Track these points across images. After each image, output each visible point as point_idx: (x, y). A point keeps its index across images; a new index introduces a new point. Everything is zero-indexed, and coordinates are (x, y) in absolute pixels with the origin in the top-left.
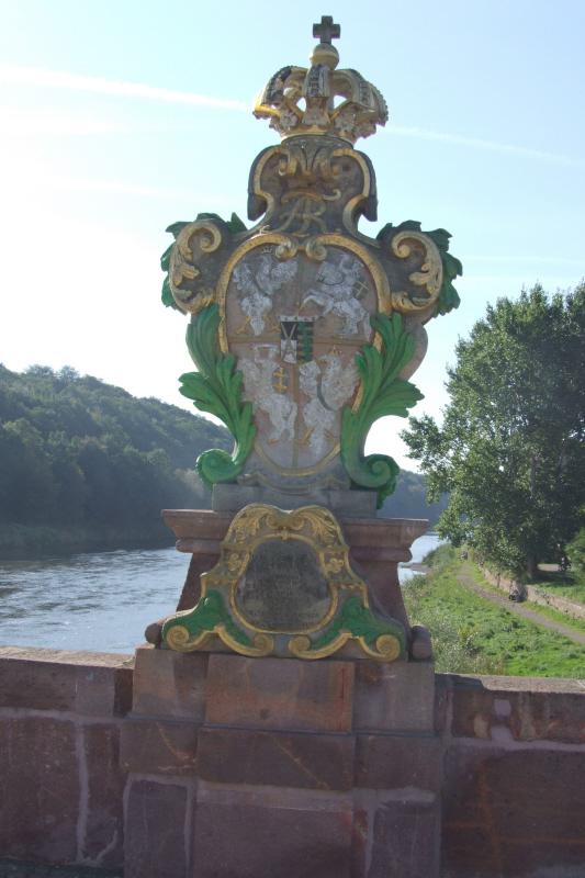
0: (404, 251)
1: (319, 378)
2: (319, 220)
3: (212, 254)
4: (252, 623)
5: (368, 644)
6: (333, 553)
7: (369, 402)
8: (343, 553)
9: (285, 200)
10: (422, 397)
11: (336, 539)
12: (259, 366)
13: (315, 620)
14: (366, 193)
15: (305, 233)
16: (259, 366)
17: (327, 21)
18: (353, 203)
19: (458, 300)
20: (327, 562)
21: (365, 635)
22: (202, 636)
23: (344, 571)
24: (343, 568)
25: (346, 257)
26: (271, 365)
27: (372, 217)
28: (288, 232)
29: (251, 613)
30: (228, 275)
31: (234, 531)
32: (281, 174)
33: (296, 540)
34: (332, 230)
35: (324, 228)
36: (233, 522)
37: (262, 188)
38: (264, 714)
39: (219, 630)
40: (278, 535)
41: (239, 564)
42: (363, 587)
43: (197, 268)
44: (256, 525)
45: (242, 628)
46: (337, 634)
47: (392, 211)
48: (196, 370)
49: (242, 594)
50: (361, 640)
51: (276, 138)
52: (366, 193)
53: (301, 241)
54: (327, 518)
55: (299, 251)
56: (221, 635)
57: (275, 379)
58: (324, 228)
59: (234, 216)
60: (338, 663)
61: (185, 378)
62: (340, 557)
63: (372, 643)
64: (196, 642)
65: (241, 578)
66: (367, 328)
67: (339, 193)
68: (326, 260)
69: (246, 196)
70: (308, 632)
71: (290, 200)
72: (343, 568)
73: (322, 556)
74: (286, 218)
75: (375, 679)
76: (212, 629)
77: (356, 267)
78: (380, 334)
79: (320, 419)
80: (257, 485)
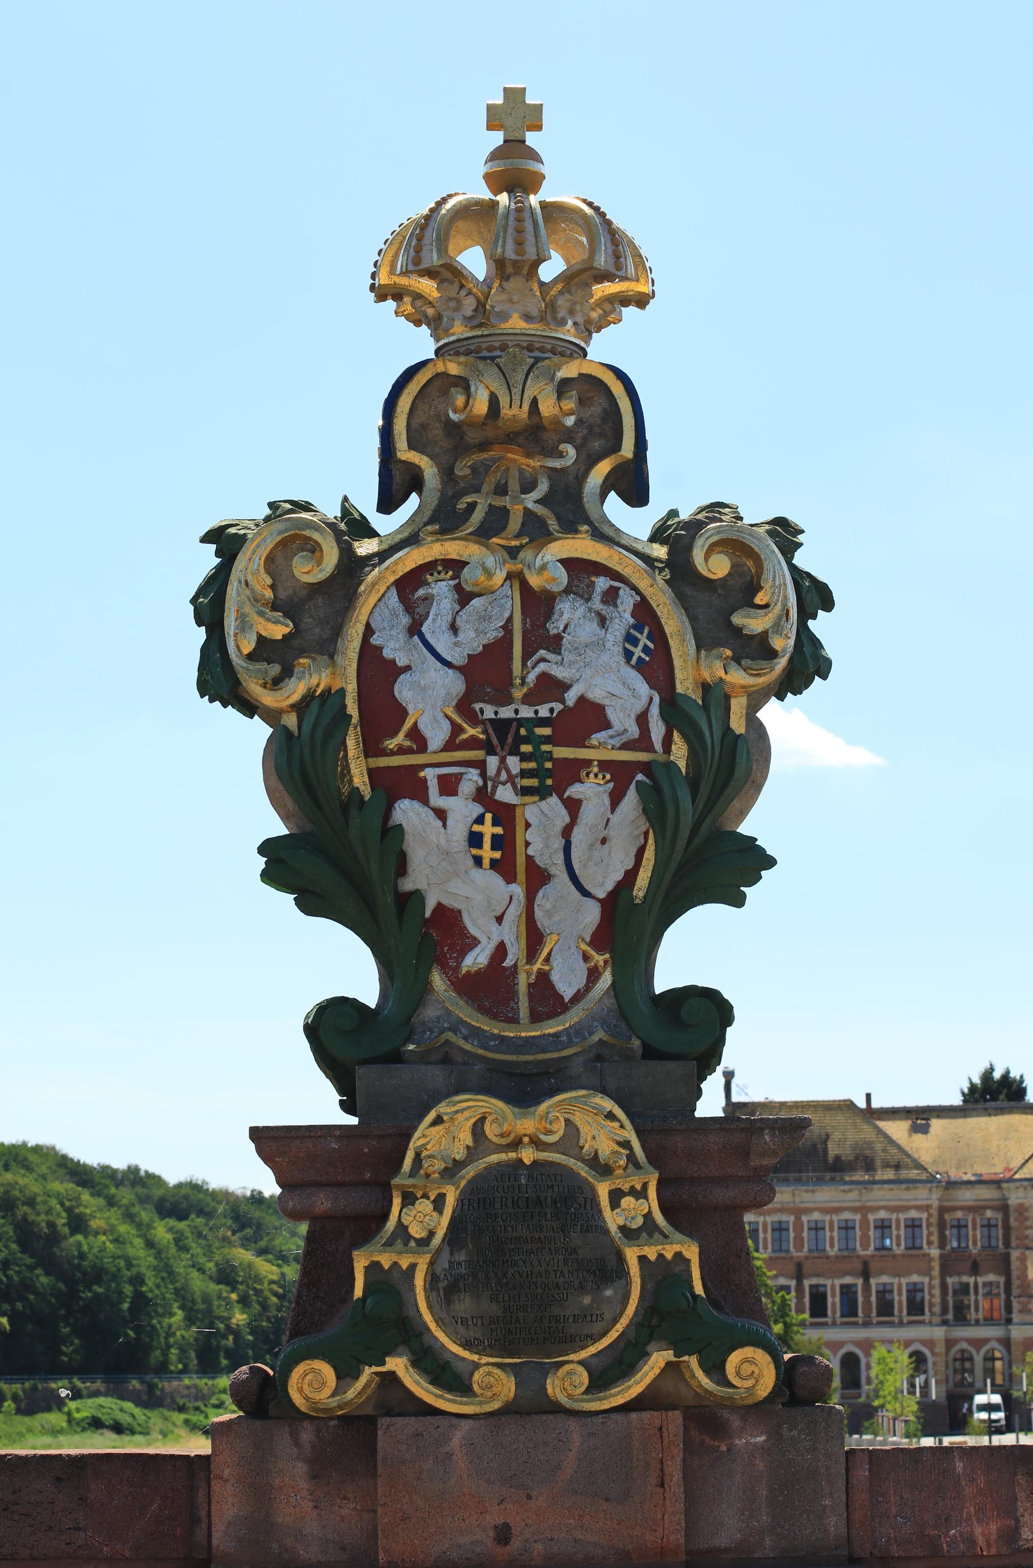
0: (718, 567)
1: (567, 832)
2: (540, 510)
3: (316, 589)
4: (467, 1345)
5: (707, 1372)
6: (626, 1187)
7: (668, 877)
8: (645, 1186)
9: (462, 470)
10: (770, 862)
11: (632, 1158)
12: (441, 814)
13: (597, 1327)
14: (627, 449)
15: (517, 536)
16: (441, 814)
17: (514, 95)
18: (603, 469)
19: (828, 663)
20: (615, 1204)
21: (699, 1352)
22: (363, 1379)
23: (649, 1225)
24: (648, 1216)
25: (602, 583)
26: (462, 809)
27: (637, 494)
28: (484, 534)
29: (464, 1321)
30: (360, 628)
31: (418, 1155)
32: (453, 416)
33: (552, 1164)
34: (570, 528)
35: (553, 524)
36: (418, 1134)
37: (412, 446)
38: (503, 1534)
39: (397, 1364)
40: (512, 1155)
41: (426, 1219)
42: (692, 1252)
43: (286, 615)
44: (466, 1138)
45: (446, 1356)
46: (646, 1355)
47: (677, 486)
48: (284, 831)
49: (441, 1285)
50: (693, 1361)
51: (419, 344)
52: (627, 449)
53: (513, 553)
54: (610, 1116)
55: (509, 576)
56: (401, 1373)
57: (475, 840)
58: (553, 524)
59: (346, 509)
60: (646, 1415)
61: (267, 848)
62: (640, 1194)
63: (716, 1369)
64: (351, 1394)
65: (438, 1251)
66: (657, 730)
67: (571, 451)
68: (567, 591)
69: (376, 460)
70: (584, 1354)
71: (474, 469)
72: (648, 1216)
73: (603, 1190)
74: (472, 507)
75: (724, 1448)
76: (384, 1363)
77: (627, 600)
78: (684, 736)
79: (571, 920)
80: (446, 1060)
